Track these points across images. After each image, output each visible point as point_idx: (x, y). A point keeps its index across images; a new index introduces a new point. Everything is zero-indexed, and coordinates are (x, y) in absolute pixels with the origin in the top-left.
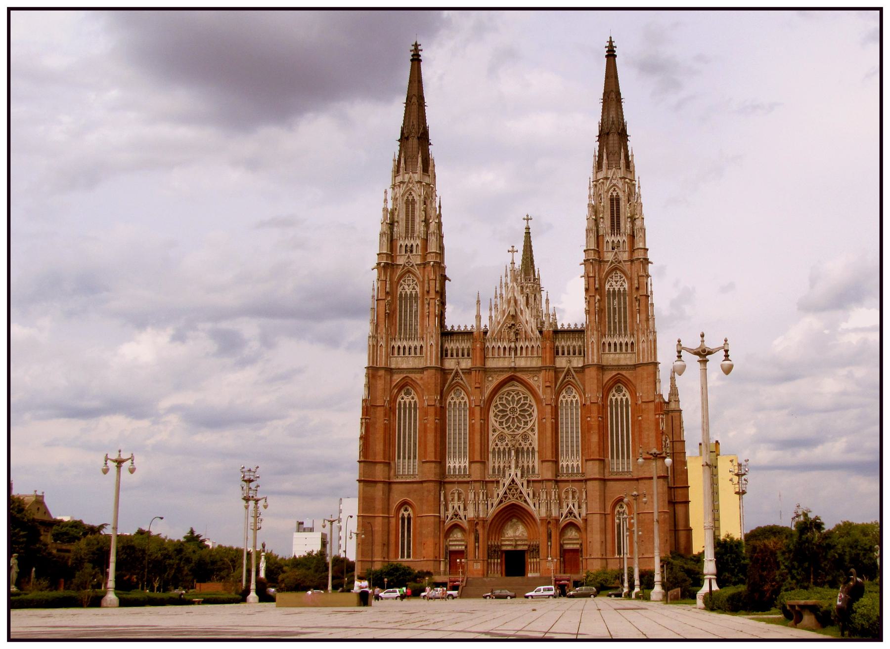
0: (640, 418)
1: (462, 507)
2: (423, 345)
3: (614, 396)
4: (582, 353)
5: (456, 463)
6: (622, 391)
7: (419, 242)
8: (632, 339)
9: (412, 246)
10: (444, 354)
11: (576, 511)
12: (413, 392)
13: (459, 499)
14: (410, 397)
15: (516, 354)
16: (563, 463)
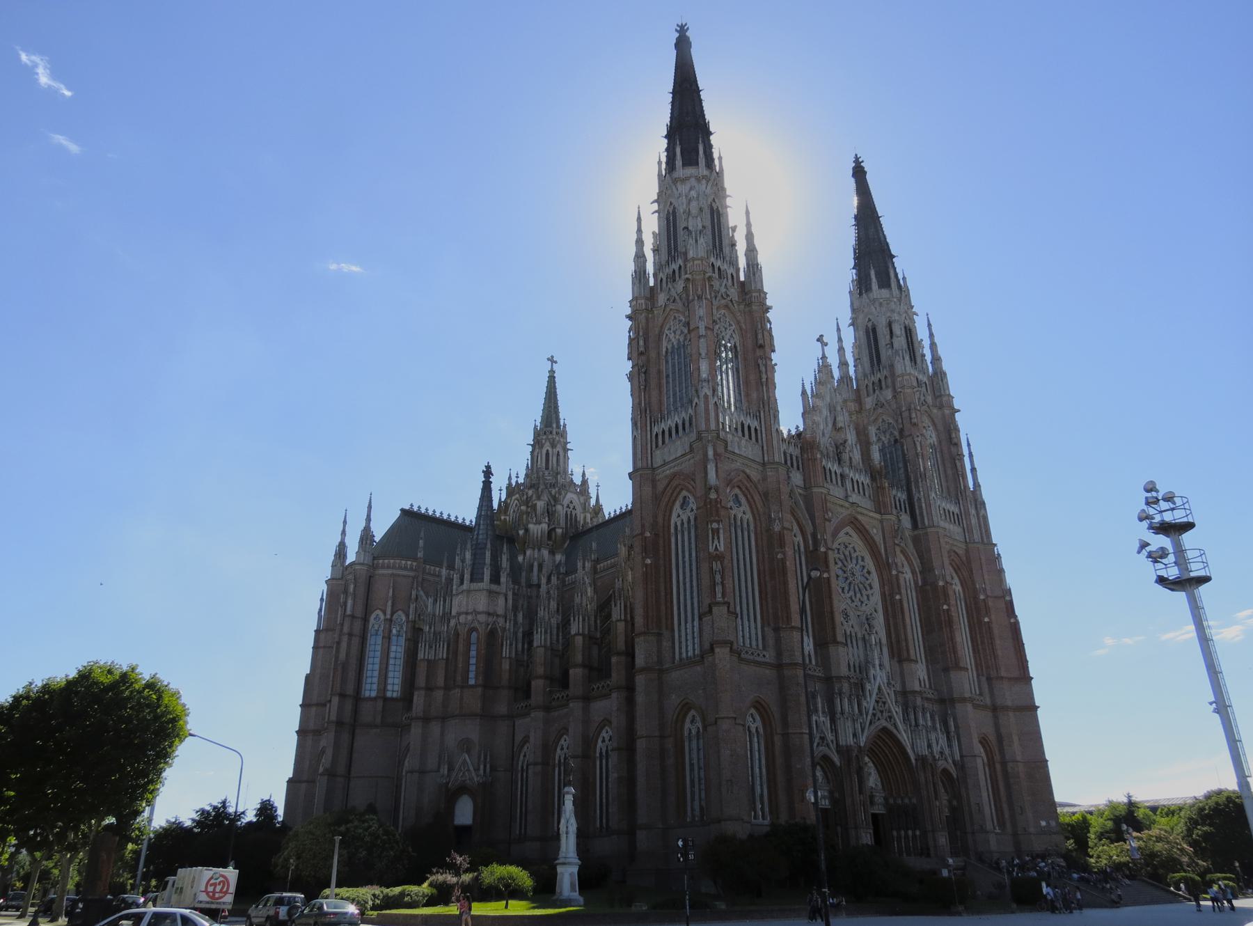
0: (986, 620)
2: (757, 427)
4: (908, 511)
11: (947, 751)
12: (743, 500)
14: (741, 509)
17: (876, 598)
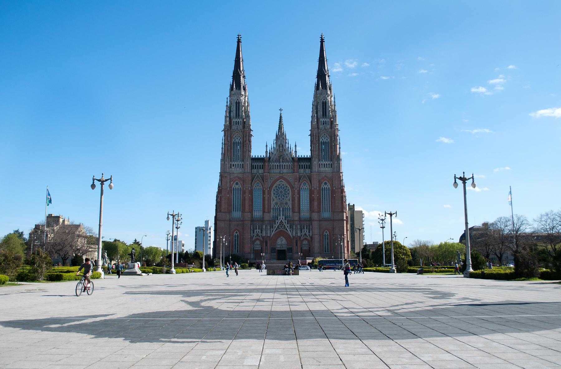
0: (334, 195)
1: (260, 232)
3: (323, 186)
5: (257, 214)
6: (327, 184)
7: (241, 120)
8: (331, 162)
9: (239, 121)
10: (252, 167)
11: (307, 234)
13: (259, 229)
14: (238, 185)
15: (282, 168)
16: (302, 214)
17: (290, 196)
